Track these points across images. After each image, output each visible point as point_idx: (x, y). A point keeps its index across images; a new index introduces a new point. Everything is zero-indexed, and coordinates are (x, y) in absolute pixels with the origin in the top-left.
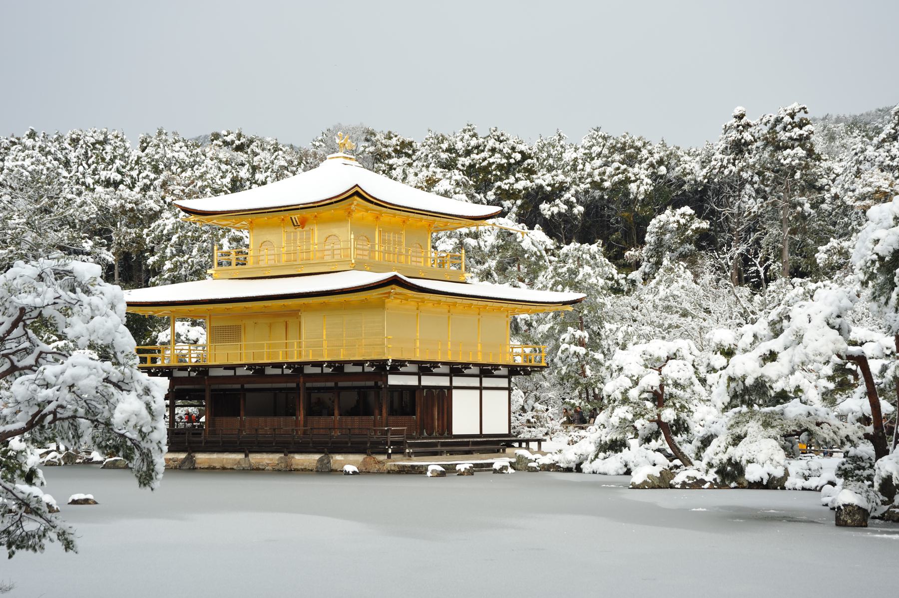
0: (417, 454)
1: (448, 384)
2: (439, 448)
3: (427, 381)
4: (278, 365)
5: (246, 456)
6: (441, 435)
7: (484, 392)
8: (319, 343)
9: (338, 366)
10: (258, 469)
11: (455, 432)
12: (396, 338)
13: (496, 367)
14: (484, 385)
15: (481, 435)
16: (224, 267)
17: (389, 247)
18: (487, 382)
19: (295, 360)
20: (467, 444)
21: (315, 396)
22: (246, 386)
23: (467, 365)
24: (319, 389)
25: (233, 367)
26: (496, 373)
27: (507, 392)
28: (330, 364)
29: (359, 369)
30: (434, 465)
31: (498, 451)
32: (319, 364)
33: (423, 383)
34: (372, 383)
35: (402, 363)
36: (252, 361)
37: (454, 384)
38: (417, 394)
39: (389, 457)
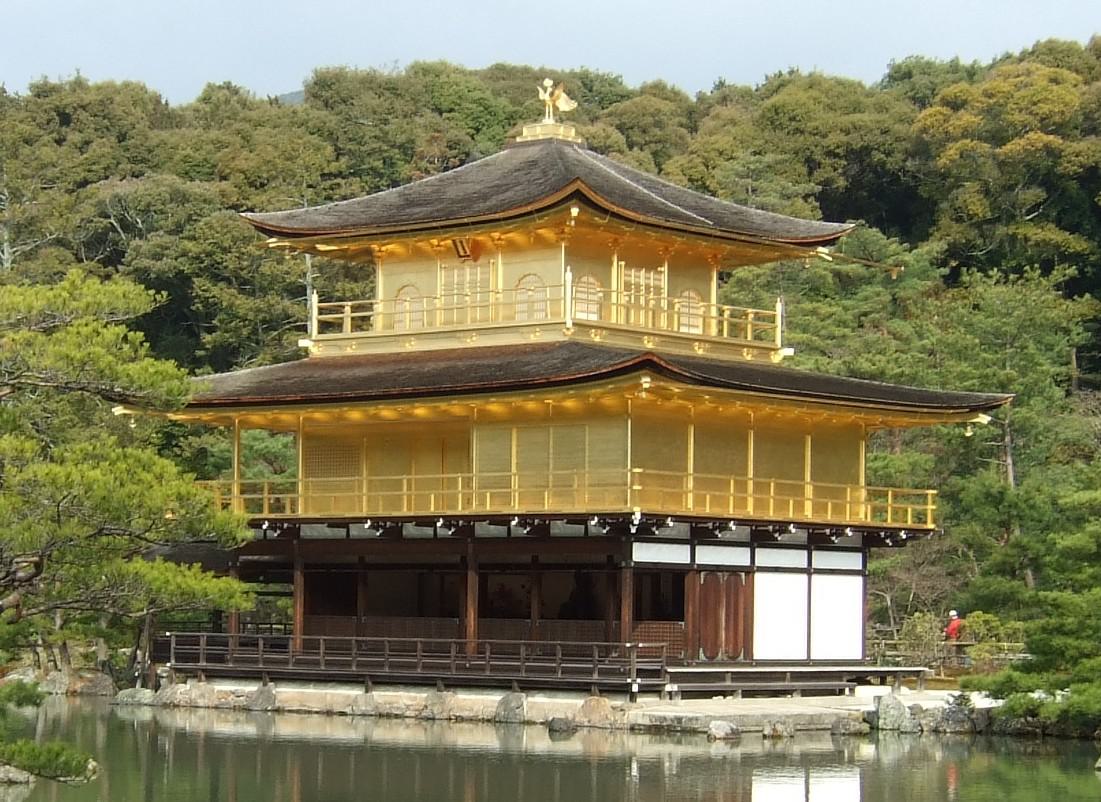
0: (687, 695)
1: (747, 563)
3: (707, 555)
4: (429, 521)
6: (733, 660)
9: (539, 525)
10: (389, 716)
11: (759, 654)
13: (839, 530)
14: (815, 565)
17: (637, 298)
18: (821, 559)
19: (460, 510)
20: (781, 676)
21: (495, 581)
22: (369, 559)
23: (782, 527)
24: (504, 567)
25: (344, 523)
27: (859, 580)
28: (525, 519)
29: (579, 529)
31: (841, 692)
32: (502, 520)
33: (699, 560)
34: (602, 558)
36: (381, 513)
37: (758, 563)
38: (688, 580)
39: (633, 697)
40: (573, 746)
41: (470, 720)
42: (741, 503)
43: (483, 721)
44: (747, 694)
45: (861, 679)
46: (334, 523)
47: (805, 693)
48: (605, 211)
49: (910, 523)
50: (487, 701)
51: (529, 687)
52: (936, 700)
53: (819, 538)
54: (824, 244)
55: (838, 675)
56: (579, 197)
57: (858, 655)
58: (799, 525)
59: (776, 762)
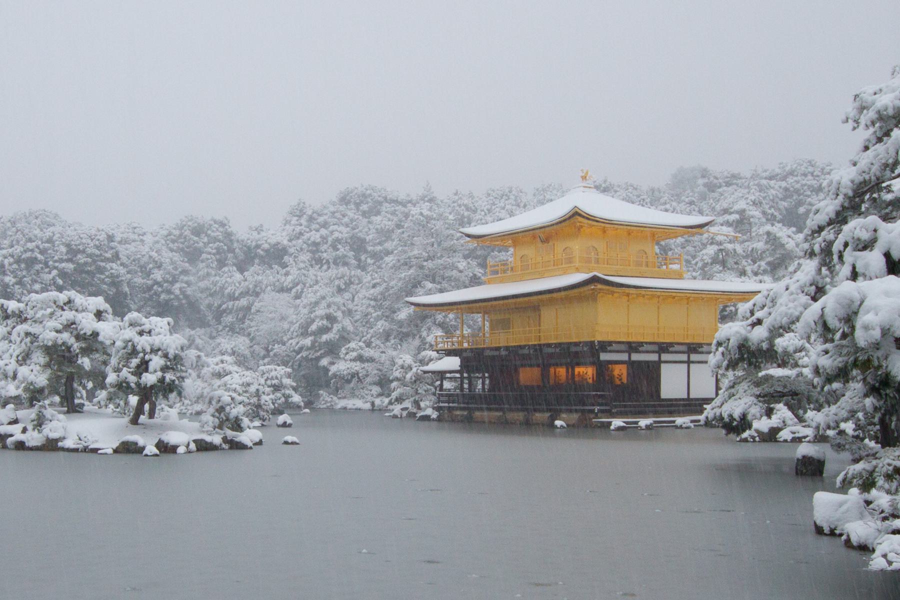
3: (635, 357)
5: (504, 413)
7: (691, 365)
8: (559, 327)
11: (664, 395)
12: (608, 322)
15: (688, 399)
16: (500, 275)
18: (694, 357)
20: (672, 405)
23: (671, 344)
25: (498, 349)
26: (700, 350)
30: (617, 422)
32: (549, 345)
35: (610, 343)
46: (491, 349)
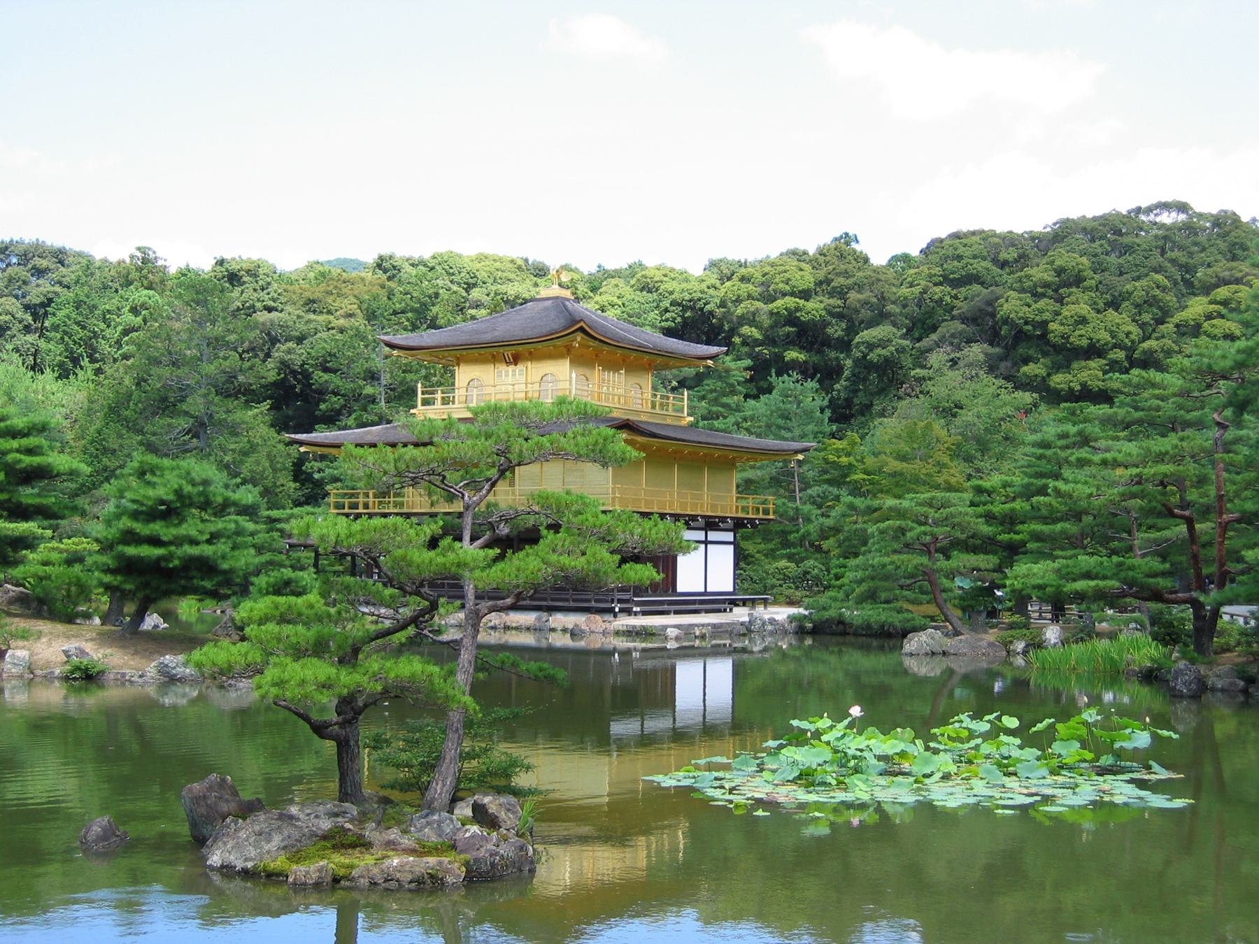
0: (645, 613)
2: (666, 607)
6: (666, 593)
11: (680, 589)
13: (723, 519)
15: (705, 593)
18: (713, 536)
20: (694, 602)
31: (725, 611)
39: (615, 616)
40: (582, 644)
41: (516, 628)
42: (671, 503)
43: (528, 629)
44: (676, 612)
45: (734, 603)
47: (707, 611)
48: (595, 339)
49: (761, 516)
50: (529, 618)
51: (551, 610)
52: (781, 613)
53: (711, 524)
54: (710, 358)
55: (724, 601)
56: (582, 330)
57: (729, 587)
58: (702, 517)
59: (687, 652)
